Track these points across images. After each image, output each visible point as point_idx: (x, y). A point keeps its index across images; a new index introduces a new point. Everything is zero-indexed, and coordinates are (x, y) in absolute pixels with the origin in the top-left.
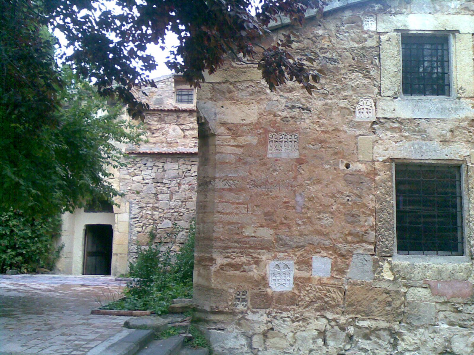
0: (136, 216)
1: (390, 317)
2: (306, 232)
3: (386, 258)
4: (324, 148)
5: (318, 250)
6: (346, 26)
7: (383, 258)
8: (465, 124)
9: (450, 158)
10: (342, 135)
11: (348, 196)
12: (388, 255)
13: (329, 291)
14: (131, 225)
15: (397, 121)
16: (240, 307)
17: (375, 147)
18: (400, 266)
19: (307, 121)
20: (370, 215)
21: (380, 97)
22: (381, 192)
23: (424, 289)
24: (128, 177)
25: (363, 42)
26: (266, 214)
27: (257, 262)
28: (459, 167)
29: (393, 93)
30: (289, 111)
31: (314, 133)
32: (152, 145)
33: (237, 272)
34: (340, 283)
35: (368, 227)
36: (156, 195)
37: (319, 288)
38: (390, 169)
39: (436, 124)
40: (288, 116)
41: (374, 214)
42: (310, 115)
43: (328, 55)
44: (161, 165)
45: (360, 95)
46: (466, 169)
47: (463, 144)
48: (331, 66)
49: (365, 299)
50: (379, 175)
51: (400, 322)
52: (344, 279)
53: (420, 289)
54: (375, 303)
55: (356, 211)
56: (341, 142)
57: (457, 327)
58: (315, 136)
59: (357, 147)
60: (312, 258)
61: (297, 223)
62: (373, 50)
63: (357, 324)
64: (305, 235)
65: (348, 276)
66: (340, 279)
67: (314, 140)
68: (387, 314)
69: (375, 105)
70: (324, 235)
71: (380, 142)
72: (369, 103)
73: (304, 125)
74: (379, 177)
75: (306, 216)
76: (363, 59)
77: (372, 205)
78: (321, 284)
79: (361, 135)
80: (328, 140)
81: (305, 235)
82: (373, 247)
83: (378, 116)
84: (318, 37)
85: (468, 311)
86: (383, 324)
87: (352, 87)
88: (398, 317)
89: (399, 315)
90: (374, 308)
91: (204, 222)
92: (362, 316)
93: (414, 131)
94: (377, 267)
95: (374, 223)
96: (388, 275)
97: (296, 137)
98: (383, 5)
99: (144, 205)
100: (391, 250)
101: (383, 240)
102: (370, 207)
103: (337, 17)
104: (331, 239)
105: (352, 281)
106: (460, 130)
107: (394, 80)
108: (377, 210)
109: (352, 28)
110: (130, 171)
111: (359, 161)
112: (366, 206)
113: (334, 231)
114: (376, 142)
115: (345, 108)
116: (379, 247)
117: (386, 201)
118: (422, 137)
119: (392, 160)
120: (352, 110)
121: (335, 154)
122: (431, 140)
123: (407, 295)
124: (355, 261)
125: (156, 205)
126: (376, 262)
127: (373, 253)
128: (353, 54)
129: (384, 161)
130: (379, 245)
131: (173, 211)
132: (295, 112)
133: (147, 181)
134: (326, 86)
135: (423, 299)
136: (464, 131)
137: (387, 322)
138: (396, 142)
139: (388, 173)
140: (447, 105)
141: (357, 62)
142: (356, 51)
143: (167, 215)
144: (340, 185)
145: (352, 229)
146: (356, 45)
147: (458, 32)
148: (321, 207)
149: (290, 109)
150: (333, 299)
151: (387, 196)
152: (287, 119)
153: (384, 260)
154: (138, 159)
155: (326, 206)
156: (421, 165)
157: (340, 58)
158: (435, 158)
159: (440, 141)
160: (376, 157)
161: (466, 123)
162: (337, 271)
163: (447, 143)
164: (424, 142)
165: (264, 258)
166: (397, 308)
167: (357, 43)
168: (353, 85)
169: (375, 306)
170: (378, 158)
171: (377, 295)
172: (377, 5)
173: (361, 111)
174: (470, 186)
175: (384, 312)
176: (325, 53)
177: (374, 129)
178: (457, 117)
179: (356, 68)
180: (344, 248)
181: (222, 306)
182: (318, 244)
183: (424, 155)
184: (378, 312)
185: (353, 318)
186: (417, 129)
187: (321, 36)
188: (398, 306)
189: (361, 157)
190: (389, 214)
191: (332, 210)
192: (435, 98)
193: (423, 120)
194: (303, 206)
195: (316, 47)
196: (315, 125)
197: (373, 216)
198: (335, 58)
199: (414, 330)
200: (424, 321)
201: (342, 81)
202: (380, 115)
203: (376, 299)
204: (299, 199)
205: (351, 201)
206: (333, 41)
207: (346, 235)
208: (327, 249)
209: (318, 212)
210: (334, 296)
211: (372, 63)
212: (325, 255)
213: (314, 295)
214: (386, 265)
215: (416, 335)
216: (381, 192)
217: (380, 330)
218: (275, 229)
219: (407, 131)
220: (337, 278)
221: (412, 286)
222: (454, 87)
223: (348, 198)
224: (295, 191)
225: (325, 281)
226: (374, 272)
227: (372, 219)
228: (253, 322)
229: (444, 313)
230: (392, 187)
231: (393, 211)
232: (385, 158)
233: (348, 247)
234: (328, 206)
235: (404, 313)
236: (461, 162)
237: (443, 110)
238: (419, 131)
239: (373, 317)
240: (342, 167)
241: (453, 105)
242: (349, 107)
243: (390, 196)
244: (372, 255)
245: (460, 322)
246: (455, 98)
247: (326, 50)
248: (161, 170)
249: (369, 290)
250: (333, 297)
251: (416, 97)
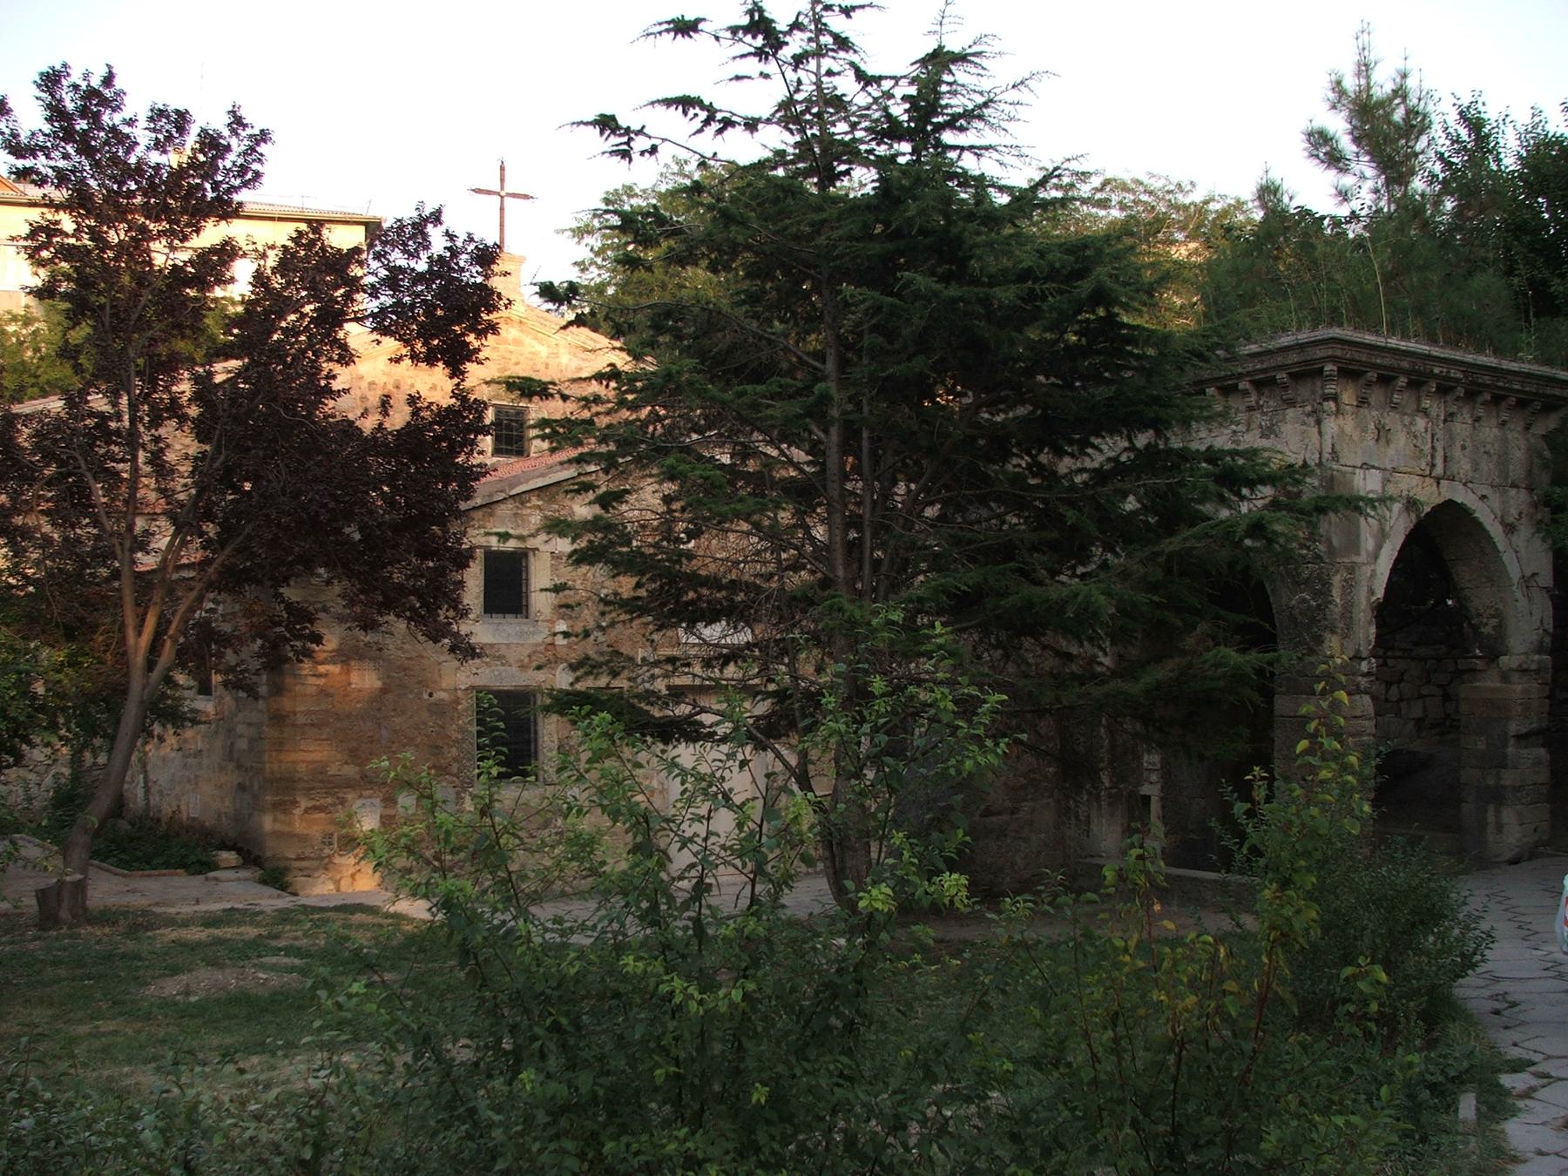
16: (327, 851)
26: (351, 751)
27: (343, 802)
33: (322, 815)
55: (439, 743)
77: (455, 735)
91: (281, 762)
126: (458, 794)
129: (467, 689)
140: (526, 629)
144: (425, 715)
165: (350, 797)
181: (308, 852)
189: (444, 685)
204: (384, 732)
218: (359, 765)
222: (533, 610)
227: (454, 750)
228: (340, 865)
234: (412, 739)
237: (521, 634)
240: (426, 696)
251: (497, 619)
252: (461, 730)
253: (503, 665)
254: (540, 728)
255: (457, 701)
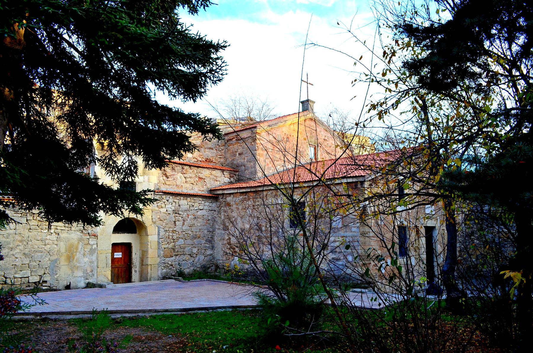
0: (163, 237)
14: (159, 243)
24: (157, 209)
32: (168, 187)
36: (175, 222)
44: (177, 201)
99: (168, 229)
110: (158, 204)
125: (175, 229)
131: (184, 233)
133: (169, 212)
143: (181, 236)
154: (164, 197)
248: (177, 205)
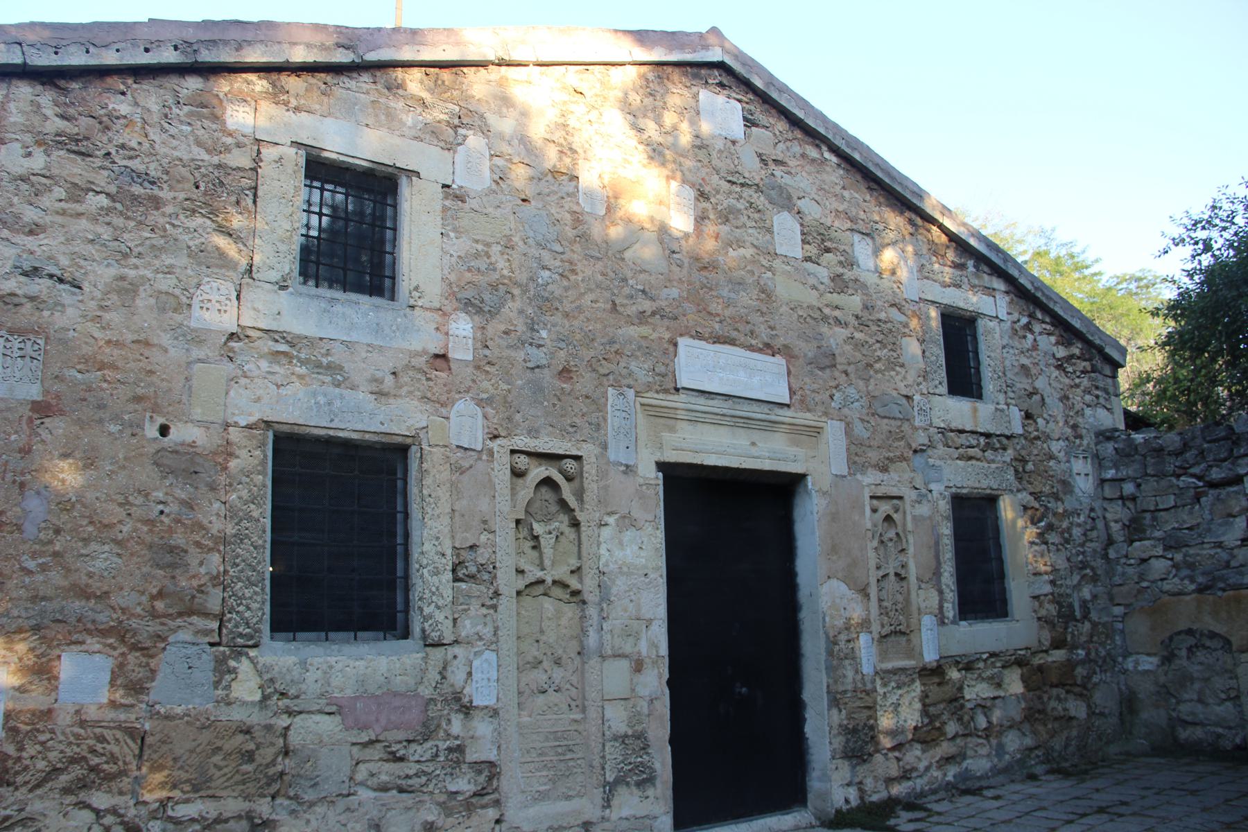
1: (251, 788)
2: (49, 592)
3: (246, 650)
4: (109, 383)
5: (75, 637)
6: (186, 109)
7: (238, 651)
8: (420, 362)
9: (388, 431)
10: (156, 356)
11: (161, 502)
12: (250, 643)
13: (101, 739)
15: (284, 338)
17: (232, 393)
18: (276, 668)
19: (70, 311)
20: (210, 550)
21: (251, 281)
22: (240, 498)
23: (327, 717)
25: (221, 152)
28: (401, 450)
29: (279, 277)
30: (23, 279)
31: (86, 343)
34: (133, 717)
35: (207, 577)
37: (74, 735)
38: (262, 445)
39: (364, 355)
40: (19, 292)
41: (222, 548)
42: (80, 298)
43: (136, 164)
45: (204, 268)
46: (419, 455)
47: (416, 403)
48: (143, 191)
49: (192, 751)
50: (237, 457)
51: (273, 798)
52: (143, 706)
53: (318, 718)
54: (217, 759)
55: (179, 539)
56: (151, 372)
57: (394, 792)
58: (86, 350)
59: (190, 387)
60: (59, 657)
61: (23, 569)
62: (242, 174)
63: (170, 813)
64: (44, 598)
65: (153, 697)
66: (132, 706)
67: (86, 360)
68: (244, 782)
69: (238, 297)
70: (98, 598)
71: (243, 381)
72: (224, 291)
73: (60, 320)
74: (238, 461)
75: (50, 548)
76: (219, 190)
77: (216, 526)
78: (83, 724)
79: (200, 361)
80: (120, 364)
81: (44, 598)
82: (215, 625)
83: (244, 323)
84: (118, 118)
85: (417, 757)
86: (233, 805)
87: (189, 247)
88: (269, 785)
89: (271, 781)
90: (213, 771)
92: (183, 792)
93: (319, 365)
94: (222, 670)
95: (222, 569)
96: (246, 687)
97: (36, 347)
98: (274, 86)
100: (258, 631)
101: (241, 608)
102: (214, 531)
103: (168, 85)
104: (113, 608)
105: (162, 711)
106: (411, 373)
107: (283, 248)
108: (228, 539)
109: (200, 117)
111: (192, 421)
112: (204, 529)
113: (122, 589)
114: (233, 380)
115: (167, 293)
116: (230, 626)
117: (250, 518)
118: (334, 379)
119: (268, 424)
120: (184, 300)
121: (138, 399)
122: (353, 388)
123: (291, 733)
124: (170, 661)
127: (217, 639)
128: (197, 175)
129: (249, 427)
130: (230, 620)
132: (40, 286)
134: (126, 236)
135: (326, 739)
136: (419, 376)
137: (245, 798)
138: (278, 386)
139: (258, 453)
141: (205, 193)
142: (203, 170)
144: (145, 474)
145: (167, 582)
146: (206, 157)
147: (418, 174)
148: (90, 529)
149: (25, 274)
150: (113, 759)
151: (252, 506)
152: (16, 300)
153: (240, 654)
155: (106, 526)
156: (329, 442)
157: (165, 177)
158: (359, 427)
159: (371, 393)
160: (233, 414)
161: (424, 359)
162: (125, 687)
163: (383, 399)
164: (337, 390)
166: (267, 766)
167: (208, 151)
168: (191, 243)
169: (215, 765)
170: (236, 419)
171: (223, 738)
172: (260, 82)
173: (206, 306)
174: (425, 492)
175: (238, 777)
176: (131, 158)
177: (232, 350)
178: (405, 345)
179: (200, 207)
180: (146, 629)
182: (79, 621)
183: (336, 420)
184: (225, 778)
185: (161, 801)
186: (325, 361)
187: (125, 117)
188: (269, 760)
189: (197, 412)
190: (255, 548)
191: (120, 537)
192: (365, 300)
193: (338, 344)
194: (43, 525)
195: (110, 141)
196: (89, 324)
197: (219, 551)
198: (153, 173)
199: (305, 812)
200: (329, 788)
201: (165, 230)
202: (246, 322)
203: (219, 749)
204: (34, 505)
205: (168, 515)
206: (152, 136)
207: (153, 598)
208: (104, 633)
209: (84, 540)
210: (115, 749)
211: (238, 203)
212: (98, 647)
213: (62, 752)
214: (244, 666)
215: (308, 821)
216: (240, 498)
217: (227, 821)
219: (303, 363)
220: (123, 705)
221: (300, 713)
222: (404, 285)
223: (161, 507)
224: (22, 485)
225: (92, 713)
226: (216, 685)
227: (216, 558)
229: (367, 765)
230: (264, 486)
231: (265, 541)
232: (253, 419)
233: (154, 627)
235: (282, 774)
236: (409, 441)
238: (329, 367)
239: (210, 792)
240: (152, 431)
241: (399, 320)
242: (177, 292)
243: (259, 506)
244: (212, 645)
245: (399, 782)
246: (404, 306)
247: (132, 153)
249: (203, 727)
250: (112, 754)
252: (232, 513)
253: (338, 385)
254: (414, 524)
255: (228, 451)
